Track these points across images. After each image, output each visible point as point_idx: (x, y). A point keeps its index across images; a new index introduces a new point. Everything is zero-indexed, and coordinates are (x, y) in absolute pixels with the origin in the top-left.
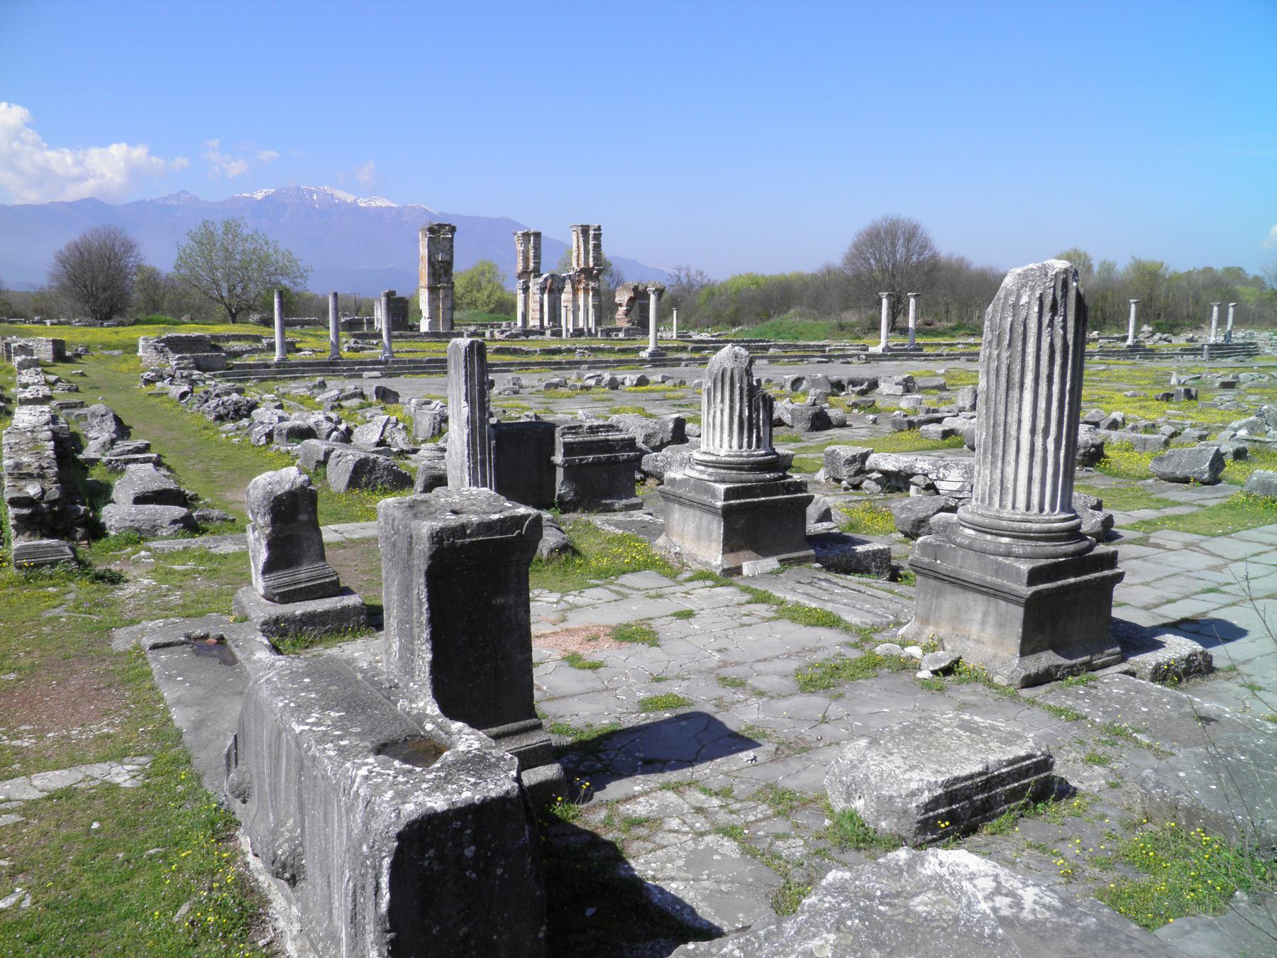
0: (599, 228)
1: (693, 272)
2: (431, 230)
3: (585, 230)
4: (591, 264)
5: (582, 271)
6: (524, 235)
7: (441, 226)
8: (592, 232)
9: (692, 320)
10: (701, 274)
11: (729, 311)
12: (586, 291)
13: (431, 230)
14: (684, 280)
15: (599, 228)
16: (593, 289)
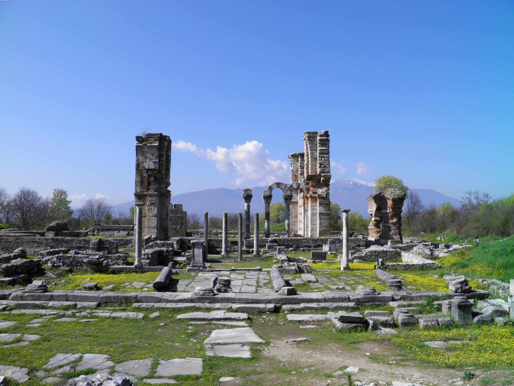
0: (326, 134)
1: (481, 196)
2: (138, 138)
3: (311, 136)
4: (318, 170)
5: (310, 178)
6: (293, 156)
7: (150, 136)
8: (319, 138)
9: (464, 230)
10: (487, 196)
11: (496, 223)
12: (314, 199)
13: (138, 138)
14: (474, 201)
15: (326, 134)
16: (320, 197)
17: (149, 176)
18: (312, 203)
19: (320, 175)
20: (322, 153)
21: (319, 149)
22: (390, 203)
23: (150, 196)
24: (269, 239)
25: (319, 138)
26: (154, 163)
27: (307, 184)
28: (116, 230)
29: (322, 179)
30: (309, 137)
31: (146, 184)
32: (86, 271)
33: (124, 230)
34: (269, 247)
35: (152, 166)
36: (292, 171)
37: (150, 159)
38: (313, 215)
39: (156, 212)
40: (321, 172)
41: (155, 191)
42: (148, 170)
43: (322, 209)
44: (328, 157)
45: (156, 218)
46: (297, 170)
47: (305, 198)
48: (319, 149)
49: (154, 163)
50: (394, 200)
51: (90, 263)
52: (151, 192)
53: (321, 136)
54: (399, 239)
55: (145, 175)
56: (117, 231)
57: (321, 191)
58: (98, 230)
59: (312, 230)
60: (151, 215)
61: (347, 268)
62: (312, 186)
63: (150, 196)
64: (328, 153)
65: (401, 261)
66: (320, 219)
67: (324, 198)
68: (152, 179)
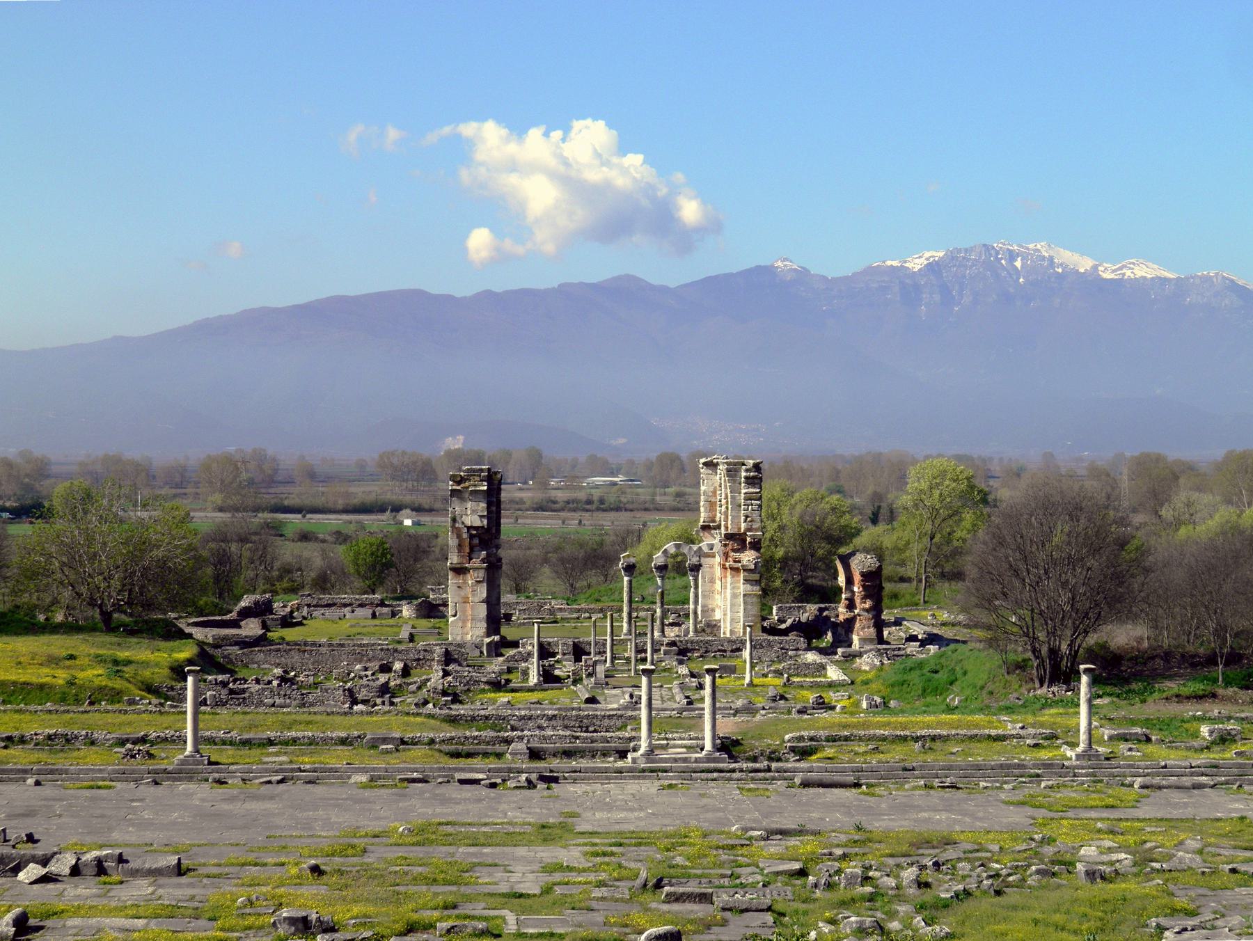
0: (757, 467)
4: (743, 526)
17: (471, 537)
18: (733, 577)
19: (745, 533)
20: (749, 498)
21: (743, 491)
22: (857, 578)
23: (475, 569)
24: (666, 640)
25: (744, 474)
26: (481, 517)
27: (725, 545)
28: (345, 605)
29: (748, 539)
30: (728, 470)
31: (467, 550)
32: (483, 691)
33: (362, 605)
34: (666, 653)
35: (477, 523)
36: (705, 493)
37: (474, 512)
38: (734, 596)
39: (485, 595)
40: (749, 530)
41: (483, 561)
42: (469, 528)
43: (749, 587)
44: (760, 506)
45: (484, 606)
46: (714, 492)
47: (724, 567)
48: (743, 491)
49: (481, 517)
50: (863, 574)
51: (488, 683)
52: (476, 562)
53: (747, 471)
54: (874, 636)
55: (465, 536)
56: (349, 609)
57: (748, 557)
58: (309, 606)
59: (732, 620)
60: (477, 600)
61: (751, 684)
62: (734, 551)
63: (475, 569)
64: (760, 499)
65: (825, 676)
66: (745, 603)
67: (750, 570)
68: (476, 541)
